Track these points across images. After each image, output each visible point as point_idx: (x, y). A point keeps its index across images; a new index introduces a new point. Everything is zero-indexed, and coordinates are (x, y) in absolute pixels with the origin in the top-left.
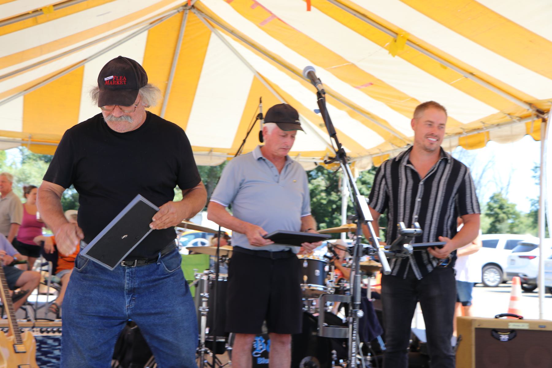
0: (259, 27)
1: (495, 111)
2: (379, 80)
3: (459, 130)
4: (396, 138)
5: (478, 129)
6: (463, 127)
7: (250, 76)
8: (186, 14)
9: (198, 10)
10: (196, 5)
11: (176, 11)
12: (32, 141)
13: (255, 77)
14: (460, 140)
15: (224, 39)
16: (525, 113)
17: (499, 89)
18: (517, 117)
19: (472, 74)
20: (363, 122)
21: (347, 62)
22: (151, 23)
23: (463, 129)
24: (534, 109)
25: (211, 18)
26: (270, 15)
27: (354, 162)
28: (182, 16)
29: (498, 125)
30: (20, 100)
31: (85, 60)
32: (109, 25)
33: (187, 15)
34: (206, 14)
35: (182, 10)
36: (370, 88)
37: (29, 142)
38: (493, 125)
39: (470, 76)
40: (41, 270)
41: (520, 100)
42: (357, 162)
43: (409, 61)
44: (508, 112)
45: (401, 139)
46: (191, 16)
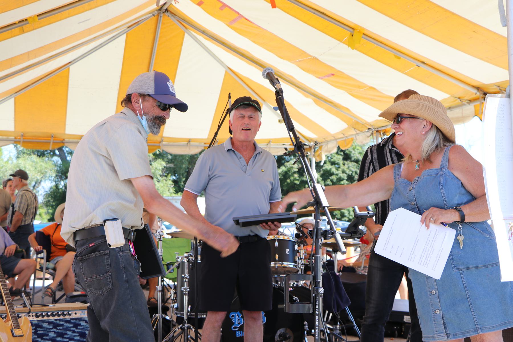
0: (229, 26)
4: (357, 123)
7: (222, 71)
8: (161, 17)
9: (171, 13)
10: (169, 9)
11: (151, 14)
12: (24, 139)
13: (226, 71)
15: (196, 38)
16: (474, 96)
18: (467, 100)
19: (423, 63)
20: (327, 110)
21: (310, 56)
22: (129, 27)
24: (481, 92)
25: (184, 20)
26: (238, 15)
27: (321, 146)
28: (158, 19)
30: (12, 101)
31: (70, 63)
32: (90, 31)
33: (162, 18)
34: (179, 17)
35: (157, 14)
36: (332, 78)
37: (22, 140)
39: (422, 65)
40: (37, 258)
41: (469, 85)
42: (323, 147)
44: (458, 97)
45: (362, 124)
46: (166, 19)
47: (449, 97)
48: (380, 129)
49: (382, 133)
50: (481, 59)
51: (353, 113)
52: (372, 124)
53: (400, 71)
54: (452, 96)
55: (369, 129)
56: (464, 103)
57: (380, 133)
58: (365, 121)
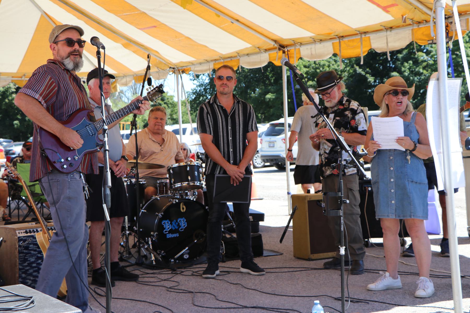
1: (249, 46)
3: (217, 57)
4: (161, 62)
5: (231, 57)
6: (221, 56)
14: (214, 64)
16: (271, 46)
17: (255, 31)
19: (238, 20)
20: (134, 52)
21: (140, 11)
23: (221, 58)
29: (248, 55)
38: (244, 54)
41: (269, 38)
42: (119, 80)
43: (190, 11)
47: (251, 47)
48: (180, 68)
49: (181, 72)
50: (290, 22)
51: (161, 55)
52: (176, 64)
53: (216, 26)
54: (253, 46)
55: (170, 67)
57: (180, 71)
58: (170, 61)
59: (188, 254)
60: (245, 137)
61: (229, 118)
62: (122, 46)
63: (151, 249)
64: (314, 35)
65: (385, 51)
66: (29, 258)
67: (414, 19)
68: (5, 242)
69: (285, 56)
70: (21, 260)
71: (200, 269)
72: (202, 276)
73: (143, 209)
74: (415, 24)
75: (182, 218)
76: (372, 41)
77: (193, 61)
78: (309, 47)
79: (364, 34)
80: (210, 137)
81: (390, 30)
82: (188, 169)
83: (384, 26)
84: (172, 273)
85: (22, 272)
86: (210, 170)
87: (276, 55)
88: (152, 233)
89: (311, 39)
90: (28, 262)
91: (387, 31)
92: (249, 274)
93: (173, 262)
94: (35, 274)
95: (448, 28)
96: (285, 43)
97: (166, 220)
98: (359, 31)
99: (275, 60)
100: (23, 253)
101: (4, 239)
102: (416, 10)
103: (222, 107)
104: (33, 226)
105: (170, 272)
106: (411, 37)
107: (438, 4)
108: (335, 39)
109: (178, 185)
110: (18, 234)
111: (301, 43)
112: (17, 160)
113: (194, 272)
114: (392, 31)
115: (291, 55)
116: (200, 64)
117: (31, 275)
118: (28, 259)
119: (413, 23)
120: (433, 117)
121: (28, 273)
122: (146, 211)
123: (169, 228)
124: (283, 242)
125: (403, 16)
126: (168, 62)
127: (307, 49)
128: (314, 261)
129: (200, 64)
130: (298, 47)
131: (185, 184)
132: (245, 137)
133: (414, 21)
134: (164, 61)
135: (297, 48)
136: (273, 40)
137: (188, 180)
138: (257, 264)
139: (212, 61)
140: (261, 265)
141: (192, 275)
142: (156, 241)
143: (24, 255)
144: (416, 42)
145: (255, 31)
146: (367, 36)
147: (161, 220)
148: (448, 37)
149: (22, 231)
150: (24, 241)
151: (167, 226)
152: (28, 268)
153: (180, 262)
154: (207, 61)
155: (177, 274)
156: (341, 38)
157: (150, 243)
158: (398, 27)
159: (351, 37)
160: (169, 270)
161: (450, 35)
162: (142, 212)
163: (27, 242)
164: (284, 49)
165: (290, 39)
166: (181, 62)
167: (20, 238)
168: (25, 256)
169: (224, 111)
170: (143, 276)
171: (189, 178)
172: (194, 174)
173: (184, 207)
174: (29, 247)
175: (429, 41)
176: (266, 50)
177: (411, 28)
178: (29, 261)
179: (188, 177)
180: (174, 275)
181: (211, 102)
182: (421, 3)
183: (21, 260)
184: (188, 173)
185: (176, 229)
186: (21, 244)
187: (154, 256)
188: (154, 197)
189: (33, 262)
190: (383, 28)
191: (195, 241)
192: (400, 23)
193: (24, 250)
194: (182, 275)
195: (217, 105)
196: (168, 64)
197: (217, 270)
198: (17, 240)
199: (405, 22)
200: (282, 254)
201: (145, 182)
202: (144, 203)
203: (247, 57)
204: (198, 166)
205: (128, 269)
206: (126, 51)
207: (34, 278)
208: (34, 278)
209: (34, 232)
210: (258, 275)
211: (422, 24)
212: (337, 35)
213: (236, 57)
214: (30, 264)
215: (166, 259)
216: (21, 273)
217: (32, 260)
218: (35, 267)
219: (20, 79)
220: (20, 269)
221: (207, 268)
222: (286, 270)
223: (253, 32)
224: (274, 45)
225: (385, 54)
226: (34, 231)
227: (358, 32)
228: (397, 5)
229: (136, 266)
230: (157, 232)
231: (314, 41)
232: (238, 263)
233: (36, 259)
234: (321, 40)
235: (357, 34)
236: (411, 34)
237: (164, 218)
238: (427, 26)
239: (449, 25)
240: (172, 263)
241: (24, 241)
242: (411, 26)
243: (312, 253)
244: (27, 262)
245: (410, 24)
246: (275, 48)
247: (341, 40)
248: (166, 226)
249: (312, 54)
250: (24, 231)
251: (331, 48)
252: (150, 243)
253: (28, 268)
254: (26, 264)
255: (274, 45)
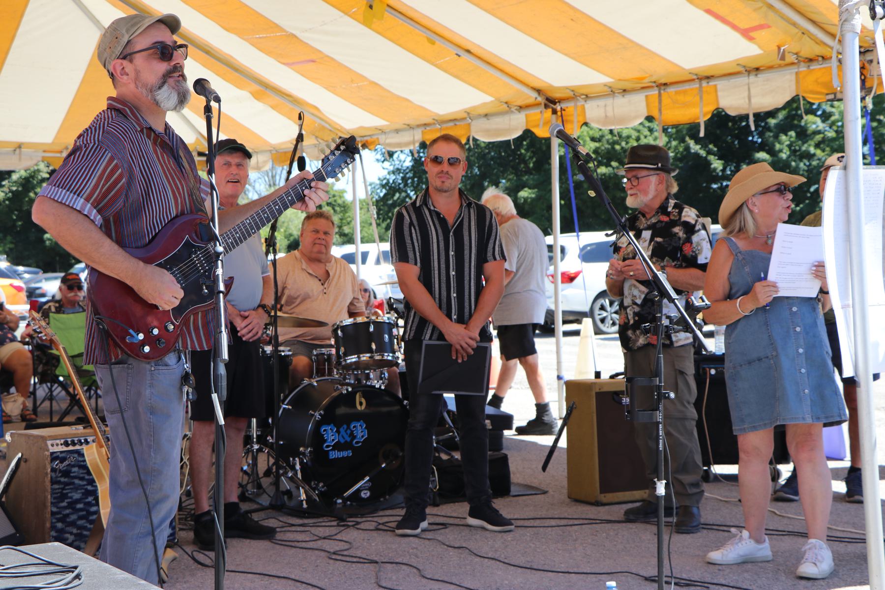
1: (489, 99)
2: (328, 56)
4: (323, 128)
5: (455, 120)
6: (436, 118)
16: (531, 101)
17: (501, 71)
19: (468, 51)
20: (273, 107)
23: (437, 120)
29: (486, 115)
39: (467, 54)
47: (492, 102)
50: (566, 55)
51: (323, 114)
54: (496, 99)
56: (512, 109)
58: (341, 126)
59: (370, 489)
60: (480, 271)
61: (451, 234)
62: (249, 95)
63: (299, 479)
64: (612, 80)
65: (744, 112)
66: (71, 492)
67: (801, 54)
68: (26, 461)
69: (557, 119)
70: (55, 495)
71: (391, 519)
72: (394, 531)
73: (286, 403)
74: (802, 64)
75: (358, 421)
76: (720, 94)
77: (384, 126)
78: (601, 102)
79: (707, 80)
80: (414, 270)
81: (755, 73)
82: (372, 329)
83: (744, 67)
84: (338, 525)
85: (56, 519)
86: (413, 332)
87: (539, 116)
88: (301, 449)
89: (606, 89)
90: (69, 500)
91: (749, 75)
92: (483, 528)
93: (340, 503)
94: (80, 522)
95: (865, 72)
96: (556, 95)
97: (329, 424)
98: (696, 75)
99: (537, 126)
100: (59, 482)
101: (24, 457)
102: (805, 36)
103: (438, 214)
104: (79, 432)
105: (335, 523)
106: (794, 87)
107: (847, 26)
108: (650, 90)
109: (352, 359)
110: (50, 447)
111: (587, 96)
112: (50, 306)
113: (380, 524)
114: (759, 76)
115: (569, 118)
116: (397, 131)
117: (73, 524)
118: (69, 495)
119: (799, 62)
120: (835, 239)
121: (68, 520)
122: (290, 407)
123: (333, 440)
124: (548, 469)
125: (779, 48)
126: (337, 127)
127: (598, 106)
128: (607, 507)
129: (397, 131)
130: (581, 102)
131: (365, 357)
132: (480, 271)
133: (800, 57)
134: (329, 125)
135: (579, 104)
136: (534, 89)
137: (370, 351)
138: (498, 511)
139: (418, 126)
140: (505, 513)
141: (377, 529)
142: (309, 463)
143: (61, 486)
144: (803, 97)
145: (501, 71)
146: (710, 84)
147: (318, 425)
148: (865, 89)
149: (58, 441)
150: (62, 460)
151: (331, 435)
152: (67, 511)
153: (354, 504)
154: (410, 127)
155: (348, 526)
156: (663, 88)
157: (298, 467)
158: (770, 68)
159: (681, 85)
160: (333, 519)
161: (868, 85)
162: (284, 408)
163: (66, 463)
164: (555, 107)
165: (567, 88)
166: (362, 128)
167: (55, 455)
168: (63, 489)
169: (443, 221)
170: (283, 529)
171: (374, 346)
172: (383, 338)
173: (363, 401)
174: (70, 472)
175: (827, 94)
176: (521, 108)
177: (794, 70)
178: (71, 498)
179: (370, 345)
180: (343, 528)
181: (418, 204)
182: (814, 22)
183: (55, 495)
184: (370, 337)
185: (346, 441)
186: (57, 465)
187: (306, 492)
188: (306, 382)
189: (78, 501)
190: (743, 69)
191: (383, 466)
192: (775, 60)
193: (61, 477)
194: (358, 529)
195: (429, 210)
196: (337, 132)
197: (424, 520)
198: (49, 459)
199: (783, 58)
200: (545, 493)
201: (290, 353)
202: (287, 392)
203: (485, 119)
204: (389, 323)
205: (255, 517)
206: (258, 105)
207: (79, 531)
208: (79, 531)
209: (81, 444)
210: (500, 532)
211: (815, 63)
212: (655, 82)
213: (464, 119)
214: (72, 505)
215: (327, 497)
216: (54, 521)
217: (77, 496)
218: (81, 510)
219: (58, 155)
220: (53, 513)
221: (404, 516)
222: (553, 522)
223: (498, 74)
224: (536, 98)
225: (746, 117)
226: (80, 441)
227: (695, 77)
228: (769, 27)
229: (270, 511)
230: (311, 447)
231: (611, 92)
232: (463, 508)
233: (83, 494)
234: (625, 91)
235: (693, 80)
236: (794, 83)
237: (325, 420)
238: (824, 68)
239: (867, 65)
240: (338, 506)
241: (62, 460)
242: (796, 66)
243: (601, 493)
244: (66, 501)
245: (793, 64)
246: (538, 104)
247: (662, 92)
248: (328, 436)
249: (606, 116)
250: (62, 441)
251: (644, 104)
252: (298, 467)
253: (67, 511)
254: (64, 504)
255: (536, 98)
